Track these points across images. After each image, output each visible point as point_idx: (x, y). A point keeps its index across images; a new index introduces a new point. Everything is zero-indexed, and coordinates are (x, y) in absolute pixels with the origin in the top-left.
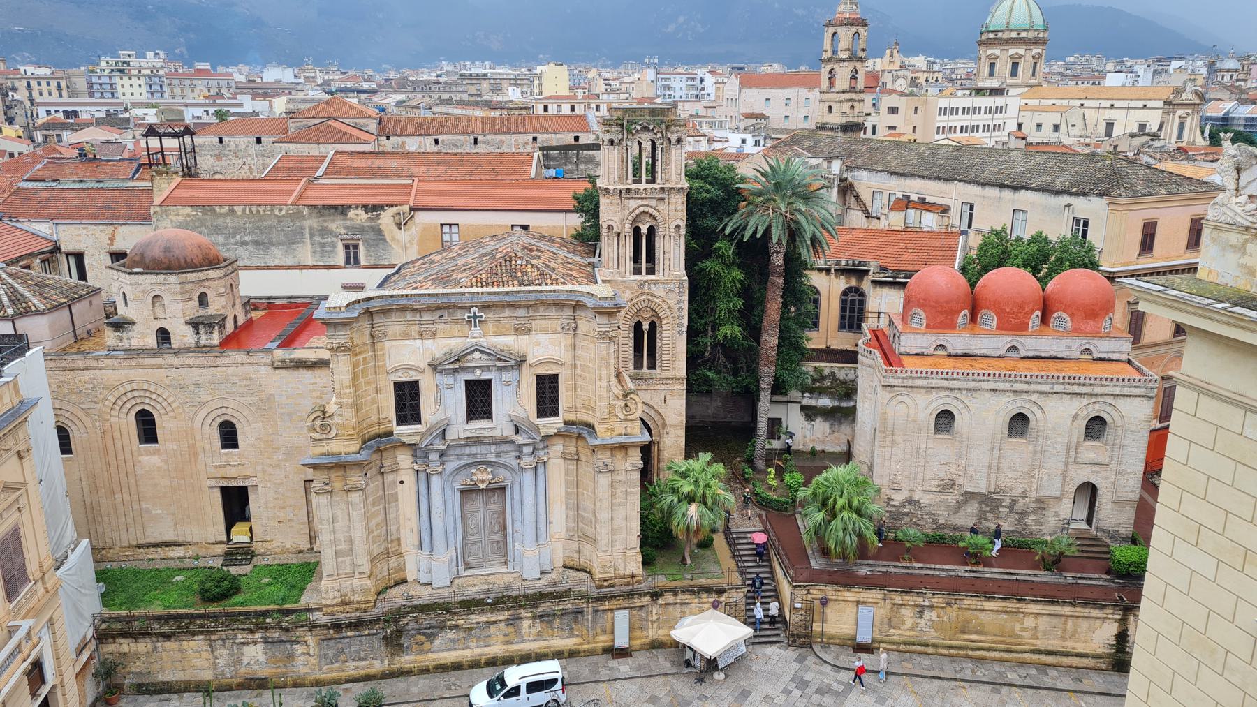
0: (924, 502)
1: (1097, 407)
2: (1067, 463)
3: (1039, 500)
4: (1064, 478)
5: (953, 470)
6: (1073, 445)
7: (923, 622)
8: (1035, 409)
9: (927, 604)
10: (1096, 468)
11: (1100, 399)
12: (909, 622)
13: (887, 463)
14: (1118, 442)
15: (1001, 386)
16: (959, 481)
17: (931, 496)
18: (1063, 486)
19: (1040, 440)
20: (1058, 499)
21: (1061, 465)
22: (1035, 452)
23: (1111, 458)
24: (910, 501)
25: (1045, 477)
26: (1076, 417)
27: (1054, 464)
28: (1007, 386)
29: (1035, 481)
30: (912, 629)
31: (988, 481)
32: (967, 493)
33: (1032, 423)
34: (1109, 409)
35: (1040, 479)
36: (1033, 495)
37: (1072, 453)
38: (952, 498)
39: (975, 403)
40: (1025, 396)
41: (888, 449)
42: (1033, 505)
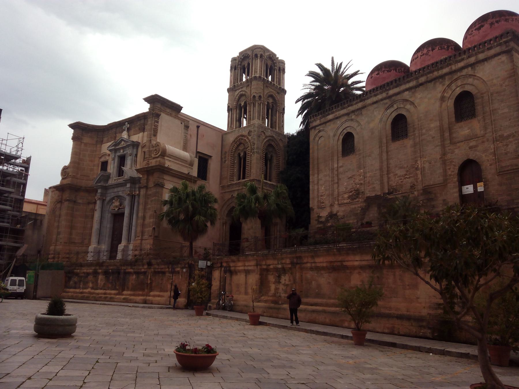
0: (340, 214)
1: (459, 83)
2: (443, 146)
3: (427, 191)
4: (444, 162)
5: (357, 181)
6: (446, 126)
7: (281, 287)
8: (408, 106)
9: (280, 266)
10: (473, 143)
11: (459, 74)
12: (273, 287)
13: (316, 187)
14: (487, 109)
15: (380, 97)
16: (362, 189)
17: (343, 209)
18: (445, 171)
19: (417, 132)
20: (444, 184)
21: (438, 149)
22: (415, 145)
23: (485, 128)
24: (332, 216)
25: (427, 165)
26: (442, 99)
27: (433, 151)
28: (384, 95)
29: (419, 172)
30: (274, 295)
31: (382, 183)
32: (368, 198)
33: (409, 120)
34: (470, 80)
35: (423, 169)
36: (420, 187)
37: (447, 134)
38: (359, 204)
39: (363, 120)
40: (399, 97)
41: (316, 176)
42: (421, 198)
